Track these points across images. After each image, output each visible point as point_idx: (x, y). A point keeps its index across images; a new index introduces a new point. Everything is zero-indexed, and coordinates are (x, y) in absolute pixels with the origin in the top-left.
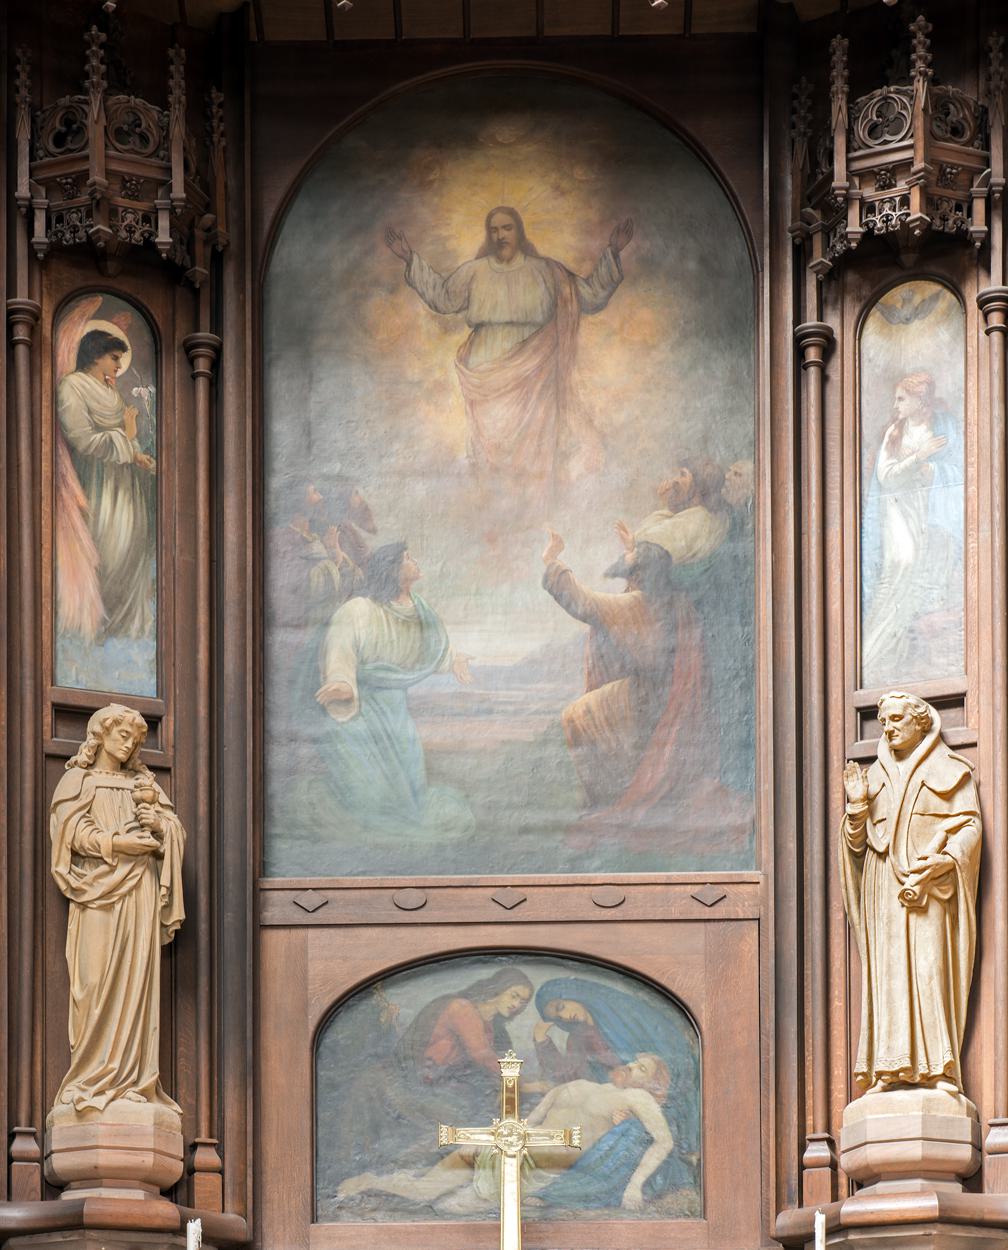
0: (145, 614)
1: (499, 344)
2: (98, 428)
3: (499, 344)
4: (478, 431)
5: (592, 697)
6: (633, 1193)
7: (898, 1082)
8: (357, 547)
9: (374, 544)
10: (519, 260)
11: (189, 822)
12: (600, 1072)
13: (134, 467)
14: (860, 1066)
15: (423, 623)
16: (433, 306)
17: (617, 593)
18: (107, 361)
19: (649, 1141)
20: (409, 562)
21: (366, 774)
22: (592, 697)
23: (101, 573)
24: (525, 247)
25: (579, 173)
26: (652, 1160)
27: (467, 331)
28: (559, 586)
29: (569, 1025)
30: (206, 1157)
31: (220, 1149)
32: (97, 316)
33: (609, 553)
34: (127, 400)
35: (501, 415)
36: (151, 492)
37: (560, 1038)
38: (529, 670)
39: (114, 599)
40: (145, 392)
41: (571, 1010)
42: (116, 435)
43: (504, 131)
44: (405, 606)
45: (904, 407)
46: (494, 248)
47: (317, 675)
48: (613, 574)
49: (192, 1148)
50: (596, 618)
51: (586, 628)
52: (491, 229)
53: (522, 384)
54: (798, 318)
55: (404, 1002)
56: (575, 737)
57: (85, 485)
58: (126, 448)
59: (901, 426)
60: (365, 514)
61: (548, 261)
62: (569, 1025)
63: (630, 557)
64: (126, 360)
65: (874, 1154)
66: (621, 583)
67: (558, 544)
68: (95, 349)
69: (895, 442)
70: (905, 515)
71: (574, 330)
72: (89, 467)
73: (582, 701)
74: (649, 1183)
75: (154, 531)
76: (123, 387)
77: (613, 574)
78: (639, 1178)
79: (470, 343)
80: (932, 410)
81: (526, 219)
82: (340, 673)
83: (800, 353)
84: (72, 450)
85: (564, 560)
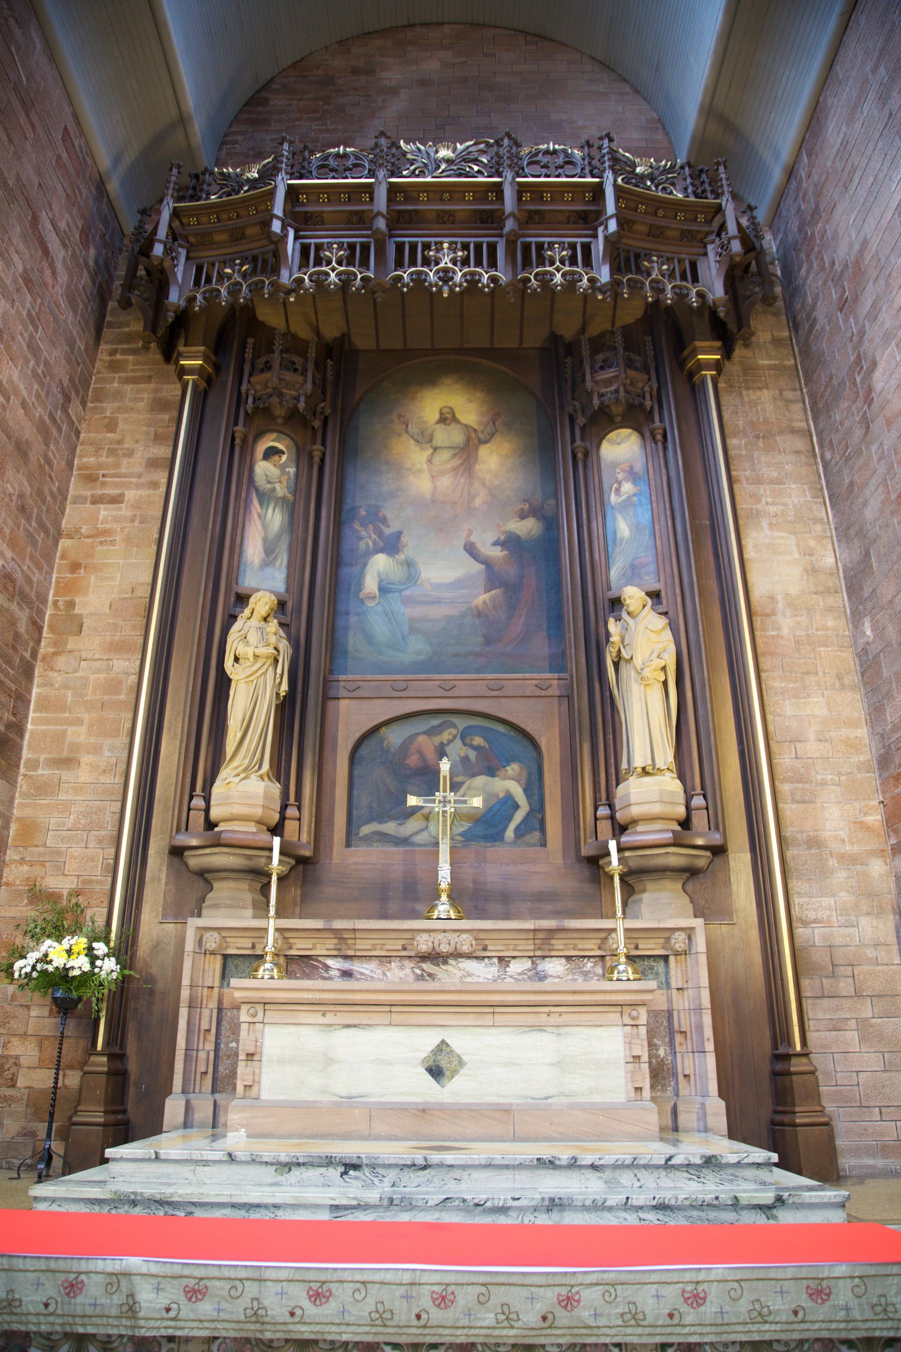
0: (283, 558)
1: (445, 455)
2: (269, 482)
3: (445, 455)
4: (435, 488)
5: (486, 596)
6: (510, 834)
7: (645, 772)
8: (380, 534)
9: (387, 531)
10: (453, 425)
11: (295, 645)
12: (491, 772)
13: (284, 499)
14: (624, 766)
15: (409, 564)
16: (417, 441)
17: (497, 553)
18: (276, 458)
19: (517, 807)
20: (404, 539)
21: (380, 628)
22: (486, 596)
23: (265, 540)
24: (455, 420)
25: (478, 395)
26: (519, 817)
27: (431, 451)
28: (471, 550)
29: (477, 748)
30: (291, 812)
31: (299, 808)
32: (273, 441)
33: (491, 536)
34: (283, 473)
35: (445, 482)
36: (291, 509)
37: (472, 755)
38: (458, 584)
39: (269, 550)
40: (292, 470)
41: (478, 741)
42: (277, 486)
43: (448, 381)
44: (401, 557)
45: (620, 476)
46: (443, 420)
47: (360, 586)
48: (495, 544)
49: (284, 807)
50: (487, 562)
51: (483, 567)
52: (441, 414)
53: (455, 470)
54: (573, 441)
55: (394, 737)
56: (479, 614)
57: (261, 504)
58: (281, 490)
59: (620, 483)
60: (384, 521)
61: (466, 426)
62: (477, 748)
63: (502, 538)
64: (284, 458)
65: (636, 811)
66: (499, 548)
67: (470, 532)
68: (271, 453)
69: (618, 491)
70: (625, 519)
71: (477, 449)
72: (265, 498)
73: (482, 599)
74: (517, 829)
75: (291, 524)
76: (282, 468)
77: (495, 544)
78: (512, 826)
79: (432, 454)
80: (633, 476)
81: (456, 410)
82: (371, 584)
83: (574, 457)
84: (257, 490)
85: (473, 539)
